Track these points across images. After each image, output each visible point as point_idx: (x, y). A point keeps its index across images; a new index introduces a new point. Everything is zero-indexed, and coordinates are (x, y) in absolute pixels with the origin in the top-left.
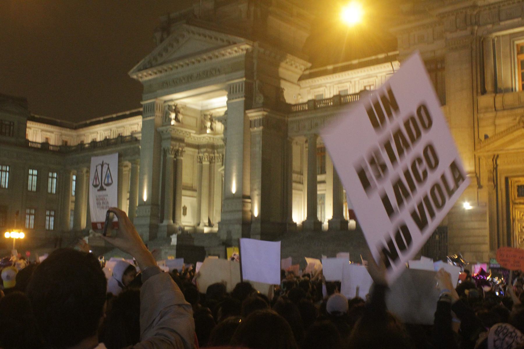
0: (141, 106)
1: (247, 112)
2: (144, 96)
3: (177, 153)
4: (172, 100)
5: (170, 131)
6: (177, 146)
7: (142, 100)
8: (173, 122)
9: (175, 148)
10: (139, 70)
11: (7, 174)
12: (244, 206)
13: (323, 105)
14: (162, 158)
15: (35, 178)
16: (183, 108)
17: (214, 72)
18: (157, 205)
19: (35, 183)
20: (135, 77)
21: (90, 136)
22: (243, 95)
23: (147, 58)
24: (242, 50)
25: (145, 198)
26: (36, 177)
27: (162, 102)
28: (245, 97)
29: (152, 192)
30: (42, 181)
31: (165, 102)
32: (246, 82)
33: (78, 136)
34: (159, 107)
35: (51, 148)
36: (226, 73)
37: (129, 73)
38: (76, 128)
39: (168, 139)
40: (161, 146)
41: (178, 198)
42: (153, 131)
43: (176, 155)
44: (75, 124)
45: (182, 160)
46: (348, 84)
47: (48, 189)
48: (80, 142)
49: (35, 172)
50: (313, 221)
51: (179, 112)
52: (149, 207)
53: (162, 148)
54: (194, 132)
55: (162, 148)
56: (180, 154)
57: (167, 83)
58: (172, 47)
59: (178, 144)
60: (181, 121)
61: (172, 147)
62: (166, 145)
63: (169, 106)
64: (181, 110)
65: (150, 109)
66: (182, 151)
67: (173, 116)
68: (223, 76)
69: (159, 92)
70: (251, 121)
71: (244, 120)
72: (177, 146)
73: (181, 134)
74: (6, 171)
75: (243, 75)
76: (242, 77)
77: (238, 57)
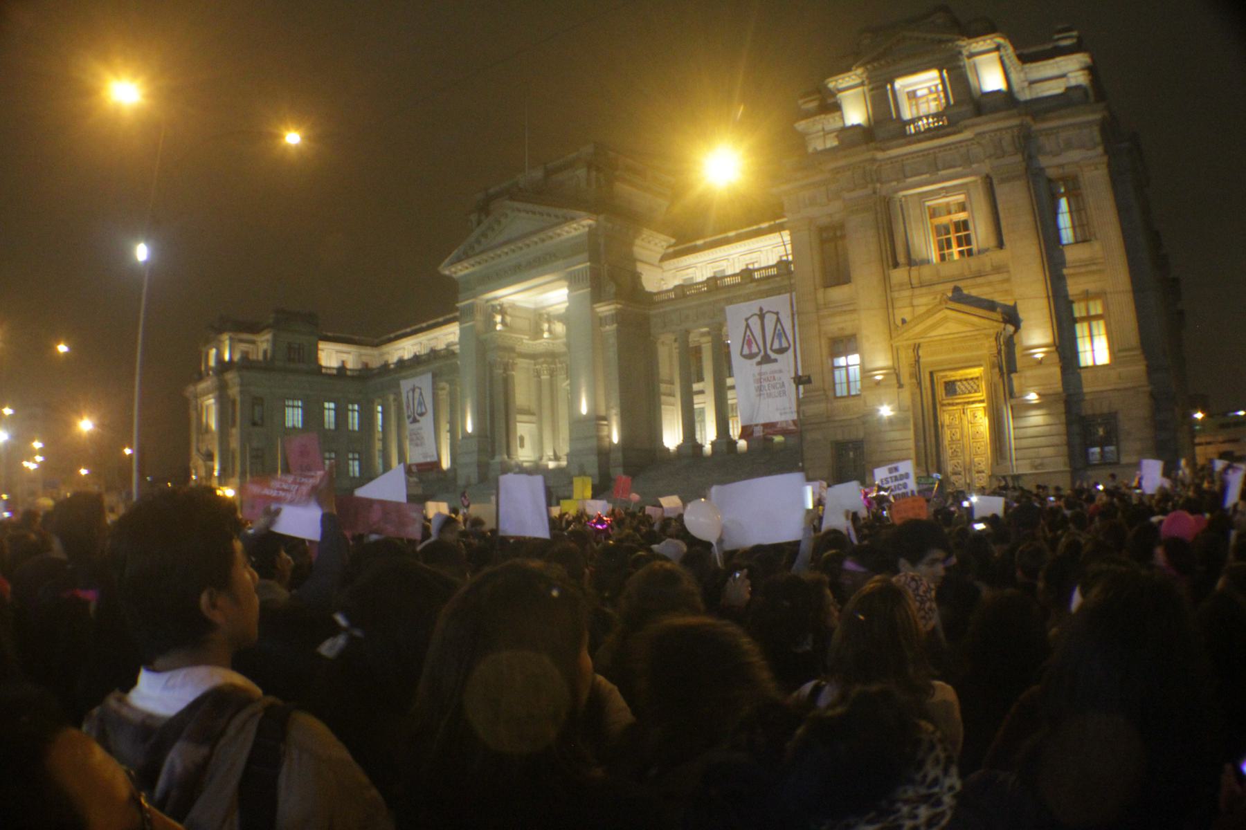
0: (457, 309)
1: (595, 306)
3: (507, 367)
4: (496, 299)
7: (457, 302)
8: (499, 327)
10: (452, 264)
15: (332, 413)
16: (510, 307)
19: (332, 420)
20: (447, 273)
24: (584, 227)
25: (469, 428)
28: (592, 287)
30: (341, 415)
31: (488, 301)
35: (349, 373)
44: (377, 341)
45: (513, 375)
47: (287, 418)
48: (383, 363)
49: (332, 405)
50: (725, 440)
54: (527, 337)
56: (510, 367)
58: (493, 230)
64: (509, 311)
74: (298, 407)
76: (585, 262)
77: (579, 236)
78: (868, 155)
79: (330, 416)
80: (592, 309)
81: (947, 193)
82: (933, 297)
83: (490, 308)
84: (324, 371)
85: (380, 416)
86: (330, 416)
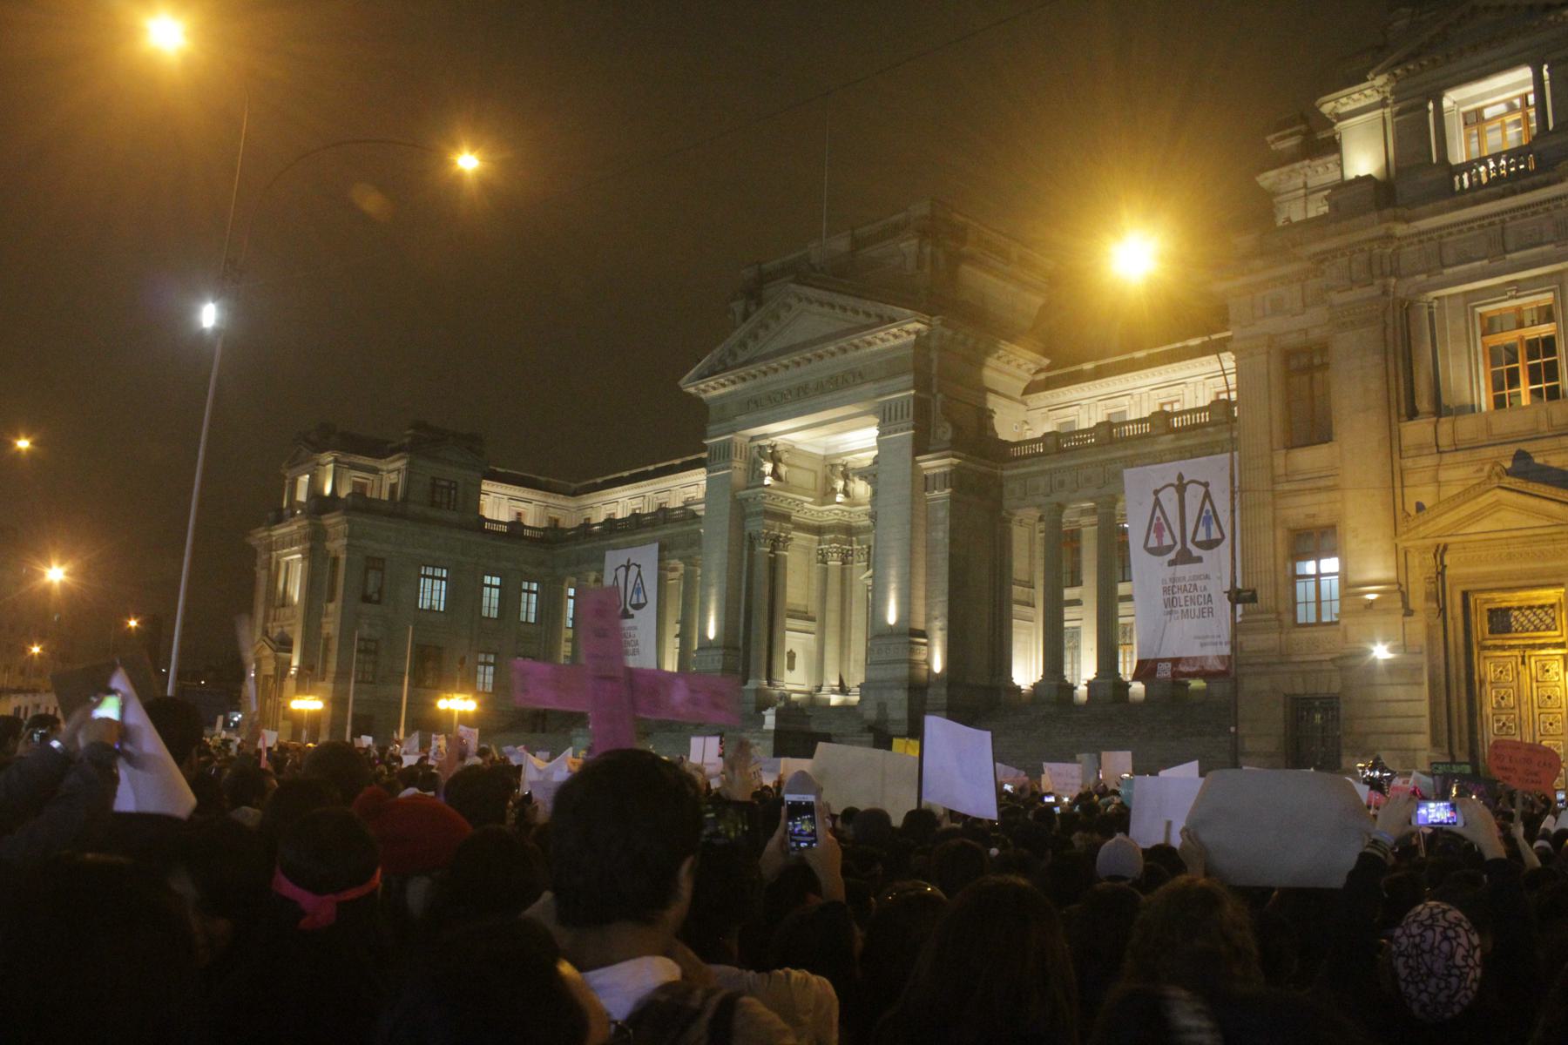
0: (704, 448)
1: (918, 458)
2: (711, 428)
3: (776, 543)
4: (765, 436)
5: (763, 498)
6: (777, 528)
7: (706, 438)
8: (768, 481)
9: (772, 532)
10: (701, 377)
11: (444, 583)
12: (912, 651)
15: (496, 592)
18: (736, 648)
19: (495, 603)
20: (692, 390)
21: (603, 510)
22: (911, 424)
23: (717, 351)
24: (908, 333)
25: (712, 633)
26: (497, 590)
27: (749, 439)
28: (914, 428)
30: (509, 599)
31: (753, 439)
32: (915, 394)
33: (581, 509)
34: (741, 451)
35: (527, 533)
36: (876, 381)
37: (682, 383)
38: (575, 494)
39: (758, 514)
40: (743, 528)
41: (777, 635)
42: (729, 499)
43: (774, 548)
44: (574, 486)
45: (785, 557)
46: (1126, 400)
48: (582, 522)
49: (496, 581)
51: (780, 461)
52: (721, 652)
53: (746, 534)
54: (811, 500)
56: (781, 544)
57: (756, 402)
58: (767, 327)
59: (778, 523)
60: (784, 478)
61: (765, 531)
62: (753, 526)
63: (760, 447)
64: (785, 457)
65: (725, 452)
66: (788, 539)
68: (867, 387)
70: (926, 477)
71: (913, 474)
72: (777, 528)
74: (441, 579)
75: (911, 383)
78: (1379, 230)
79: (491, 599)
81: (1517, 291)
82: (1475, 468)
83: (757, 450)
84: (487, 525)
85: (571, 603)
86: (491, 599)
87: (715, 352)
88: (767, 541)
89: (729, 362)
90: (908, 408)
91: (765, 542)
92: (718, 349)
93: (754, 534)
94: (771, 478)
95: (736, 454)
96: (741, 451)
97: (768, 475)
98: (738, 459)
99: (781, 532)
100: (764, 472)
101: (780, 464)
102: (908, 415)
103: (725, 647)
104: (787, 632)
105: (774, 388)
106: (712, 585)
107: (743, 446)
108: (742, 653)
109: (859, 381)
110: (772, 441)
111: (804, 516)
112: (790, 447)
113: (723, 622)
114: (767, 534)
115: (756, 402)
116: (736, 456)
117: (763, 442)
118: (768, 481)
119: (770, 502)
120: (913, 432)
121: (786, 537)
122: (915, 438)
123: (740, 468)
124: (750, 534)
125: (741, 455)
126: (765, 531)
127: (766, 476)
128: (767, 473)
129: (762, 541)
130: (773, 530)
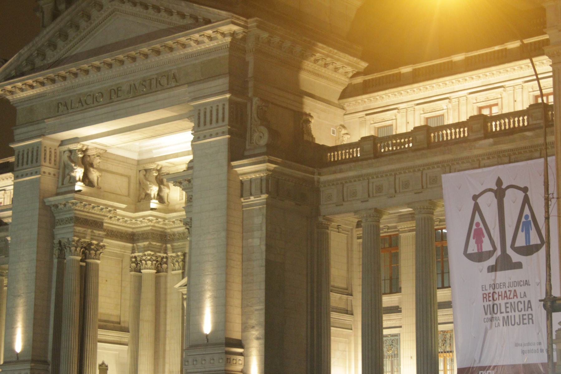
0: (11, 152)
1: (234, 163)
4: (76, 140)
5: (73, 203)
7: (13, 141)
8: (79, 186)
9: (83, 240)
12: (228, 361)
13: (349, 156)
14: (55, 261)
17: (164, 81)
18: (45, 362)
22: (226, 128)
23: (25, 51)
24: (223, 35)
25: (18, 346)
27: (58, 144)
28: (230, 132)
29: (34, 333)
31: (63, 143)
32: (230, 101)
34: (50, 156)
36: (190, 84)
39: (69, 220)
40: (53, 236)
41: (88, 346)
42: (37, 205)
45: (97, 265)
51: (92, 165)
52: (28, 366)
53: (56, 241)
54: (124, 206)
55: (56, 241)
56: (93, 252)
57: (66, 105)
58: (77, 27)
59: (90, 230)
60: (96, 184)
61: (76, 239)
63: (71, 151)
64: (97, 161)
67: (79, 172)
68: (183, 90)
69: (50, 122)
70: (242, 183)
71: (229, 180)
73: (96, 210)
75: (226, 87)
76: (223, 93)
80: (230, 168)
83: (67, 154)
87: (22, 51)
88: (78, 249)
89: (38, 62)
90: (223, 114)
91: (76, 250)
92: (26, 49)
93: (64, 241)
94: (82, 184)
95: (45, 158)
96: (50, 156)
97: (79, 180)
98: (47, 164)
99: (92, 239)
100: (74, 178)
101: (91, 169)
102: (223, 120)
103: (33, 361)
104: (99, 344)
105: (85, 90)
106: (19, 296)
107: (53, 152)
108: (50, 367)
109: (173, 84)
110: (84, 145)
111: (117, 223)
112: (102, 152)
113: (32, 335)
114: (78, 241)
115: (66, 105)
116: (45, 162)
117: (73, 147)
118: (79, 186)
119: (82, 209)
120: (228, 136)
121: (97, 245)
122: (231, 143)
123: (49, 174)
124: (60, 242)
125: (50, 160)
126: (76, 239)
127: (77, 181)
128: (77, 179)
129: (73, 249)
130: (84, 238)
